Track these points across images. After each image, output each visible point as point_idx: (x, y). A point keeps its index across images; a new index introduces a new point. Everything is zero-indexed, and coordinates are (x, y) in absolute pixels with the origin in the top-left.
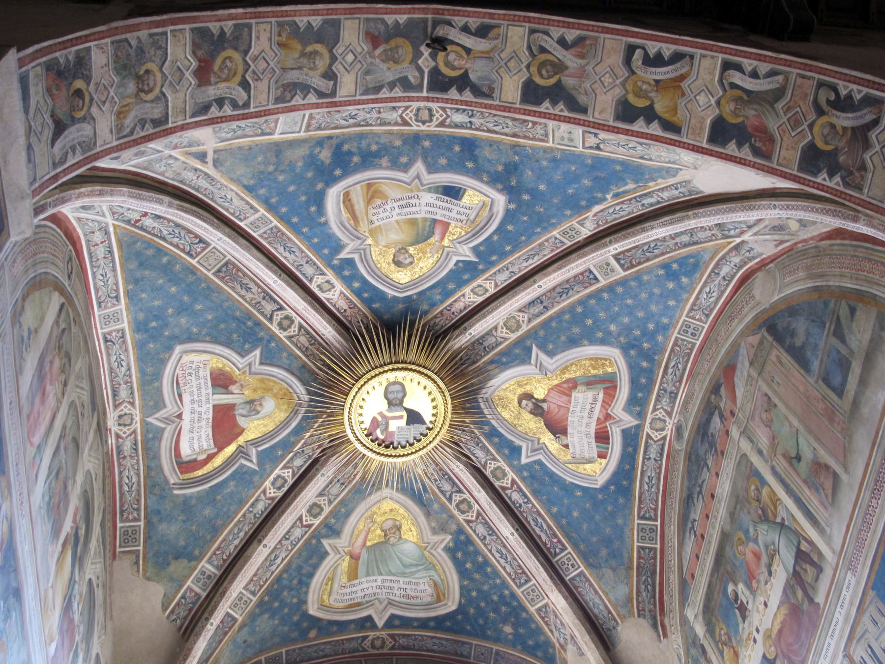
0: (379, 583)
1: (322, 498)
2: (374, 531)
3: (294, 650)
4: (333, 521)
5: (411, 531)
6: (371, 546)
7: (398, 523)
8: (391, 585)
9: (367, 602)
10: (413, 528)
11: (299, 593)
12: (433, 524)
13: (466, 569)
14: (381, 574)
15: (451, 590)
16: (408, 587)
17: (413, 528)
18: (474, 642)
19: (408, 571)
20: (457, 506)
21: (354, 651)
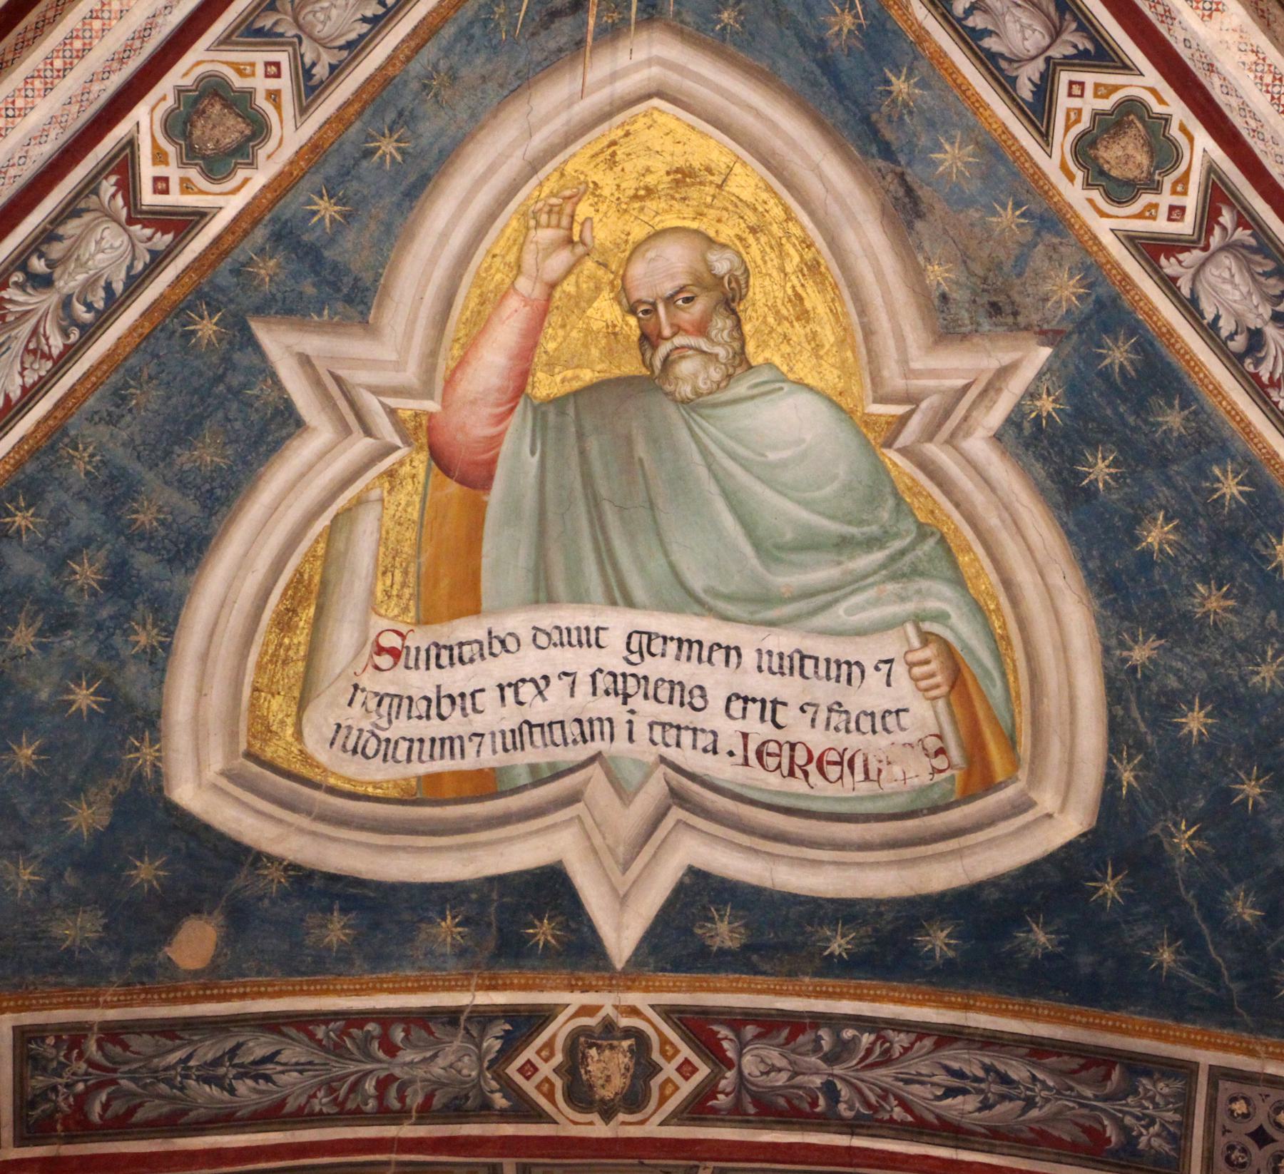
0: (613, 658)
1: (260, 57)
2: (581, 302)
3: (74, 1036)
4: (327, 209)
5: (804, 316)
6: (559, 403)
7: (722, 264)
8: (687, 672)
9: (539, 777)
10: (814, 299)
11: (108, 651)
12: (937, 274)
13: (1146, 560)
14: (621, 596)
15: (1053, 704)
16: (788, 688)
17: (814, 299)
18: (1207, 1058)
19: (787, 580)
20: (1085, 149)
21: (457, 1111)
